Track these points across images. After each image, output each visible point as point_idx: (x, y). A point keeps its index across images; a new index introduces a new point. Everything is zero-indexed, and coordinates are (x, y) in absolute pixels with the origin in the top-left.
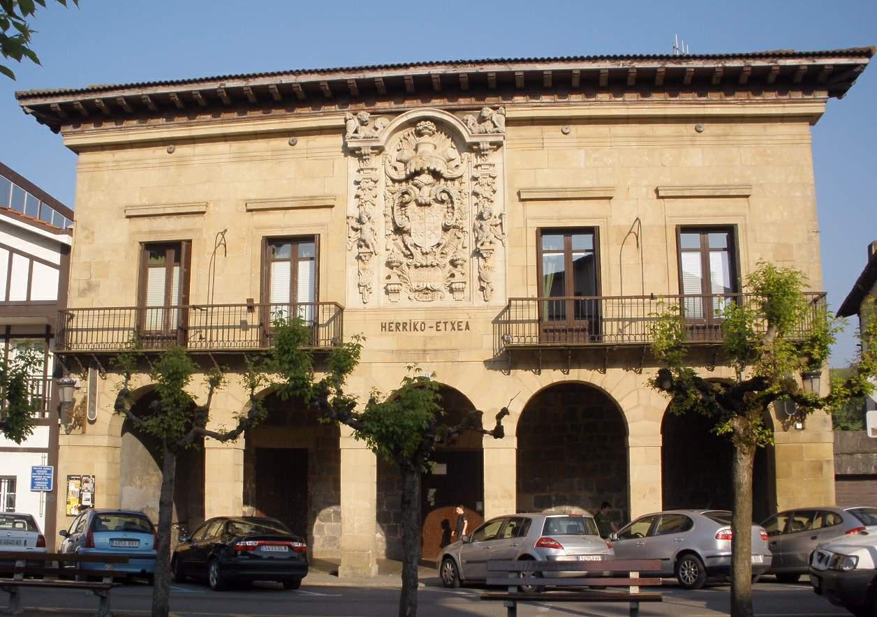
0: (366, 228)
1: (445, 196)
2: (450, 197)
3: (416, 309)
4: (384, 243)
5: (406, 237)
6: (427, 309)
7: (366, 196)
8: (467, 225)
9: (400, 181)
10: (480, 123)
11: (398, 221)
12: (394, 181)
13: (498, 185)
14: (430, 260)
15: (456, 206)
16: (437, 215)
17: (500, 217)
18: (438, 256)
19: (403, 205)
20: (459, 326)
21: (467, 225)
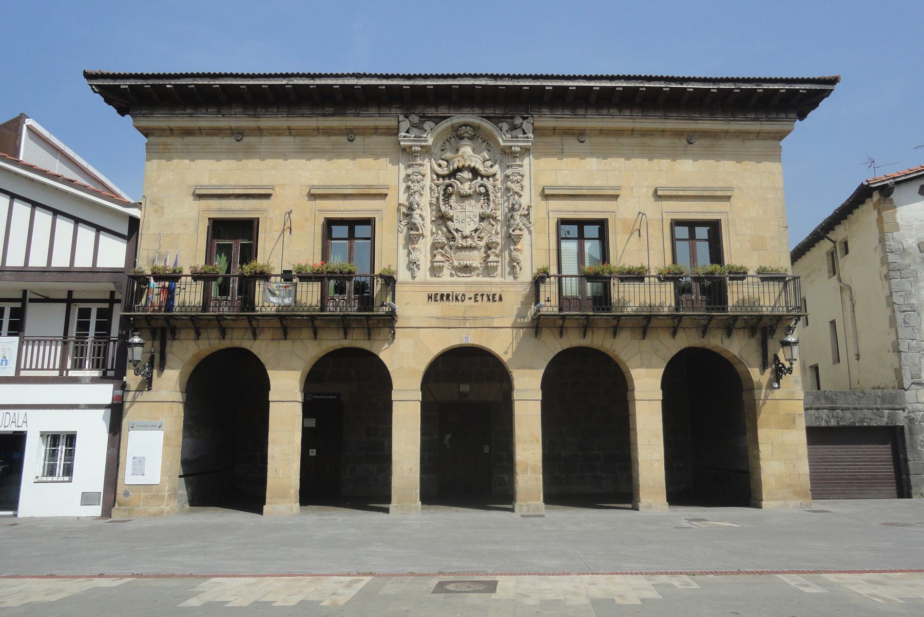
0: (416, 214)
1: (482, 190)
2: (487, 191)
3: (459, 283)
4: (427, 225)
5: (449, 223)
6: (466, 283)
7: (415, 187)
8: (499, 215)
9: (444, 177)
10: (512, 130)
11: (443, 208)
12: (438, 176)
13: (526, 182)
14: (469, 242)
15: (491, 198)
16: (474, 208)
17: (529, 207)
18: (476, 239)
19: (447, 196)
20: (494, 298)
21: (499, 215)
